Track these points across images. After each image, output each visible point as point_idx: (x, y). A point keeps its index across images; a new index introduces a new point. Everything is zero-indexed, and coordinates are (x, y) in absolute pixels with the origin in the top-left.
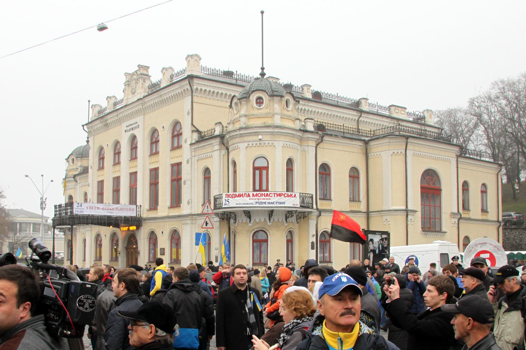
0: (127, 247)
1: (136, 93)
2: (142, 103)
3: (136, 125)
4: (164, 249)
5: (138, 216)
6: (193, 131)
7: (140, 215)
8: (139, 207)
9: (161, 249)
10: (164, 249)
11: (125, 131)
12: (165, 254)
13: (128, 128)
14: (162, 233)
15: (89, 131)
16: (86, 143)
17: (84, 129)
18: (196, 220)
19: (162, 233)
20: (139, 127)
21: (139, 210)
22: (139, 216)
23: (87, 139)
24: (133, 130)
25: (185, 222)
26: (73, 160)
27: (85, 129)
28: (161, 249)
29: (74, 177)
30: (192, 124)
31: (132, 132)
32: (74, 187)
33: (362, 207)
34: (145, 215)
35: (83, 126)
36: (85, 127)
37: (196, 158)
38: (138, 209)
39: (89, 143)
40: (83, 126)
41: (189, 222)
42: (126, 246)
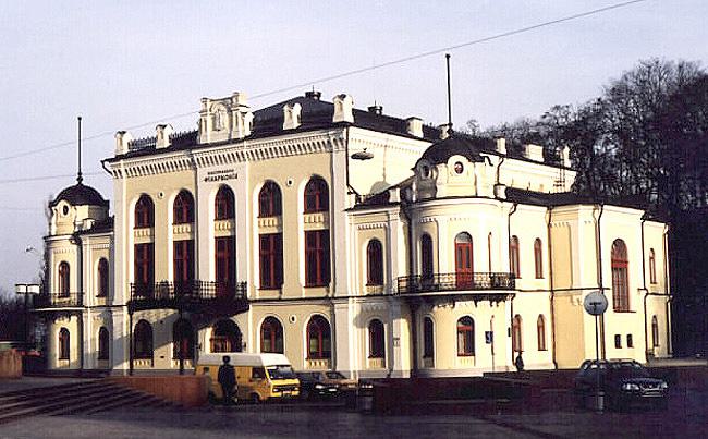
6: (349, 193)
30: (348, 185)
31: (220, 182)
33: (545, 284)
35: (103, 162)
36: (106, 163)
39: (83, 182)
40: (103, 162)
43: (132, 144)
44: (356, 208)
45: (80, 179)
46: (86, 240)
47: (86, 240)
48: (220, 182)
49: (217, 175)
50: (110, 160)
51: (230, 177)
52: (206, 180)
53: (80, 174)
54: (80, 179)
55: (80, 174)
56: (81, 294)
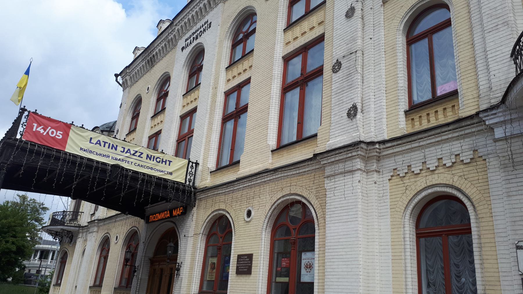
0: (153, 258)
4: (250, 257)
5: (188, 183)
7: (194, 183)
8: (194, 165)
9: (239, 257)
10: (250, 257)
12: (253, 269)
13: (189, 41)
14: (249, 213)
15: (123, 83)
17: (117, 80)
18: (379, 159)
19: (249, 213)
21: (193, 170)
22: (191, 184)
27: (118, 80)
28: (239, 257)
35: (116, 76)
38: (190, 170)
41: (359, 164)
42: (151, 255)
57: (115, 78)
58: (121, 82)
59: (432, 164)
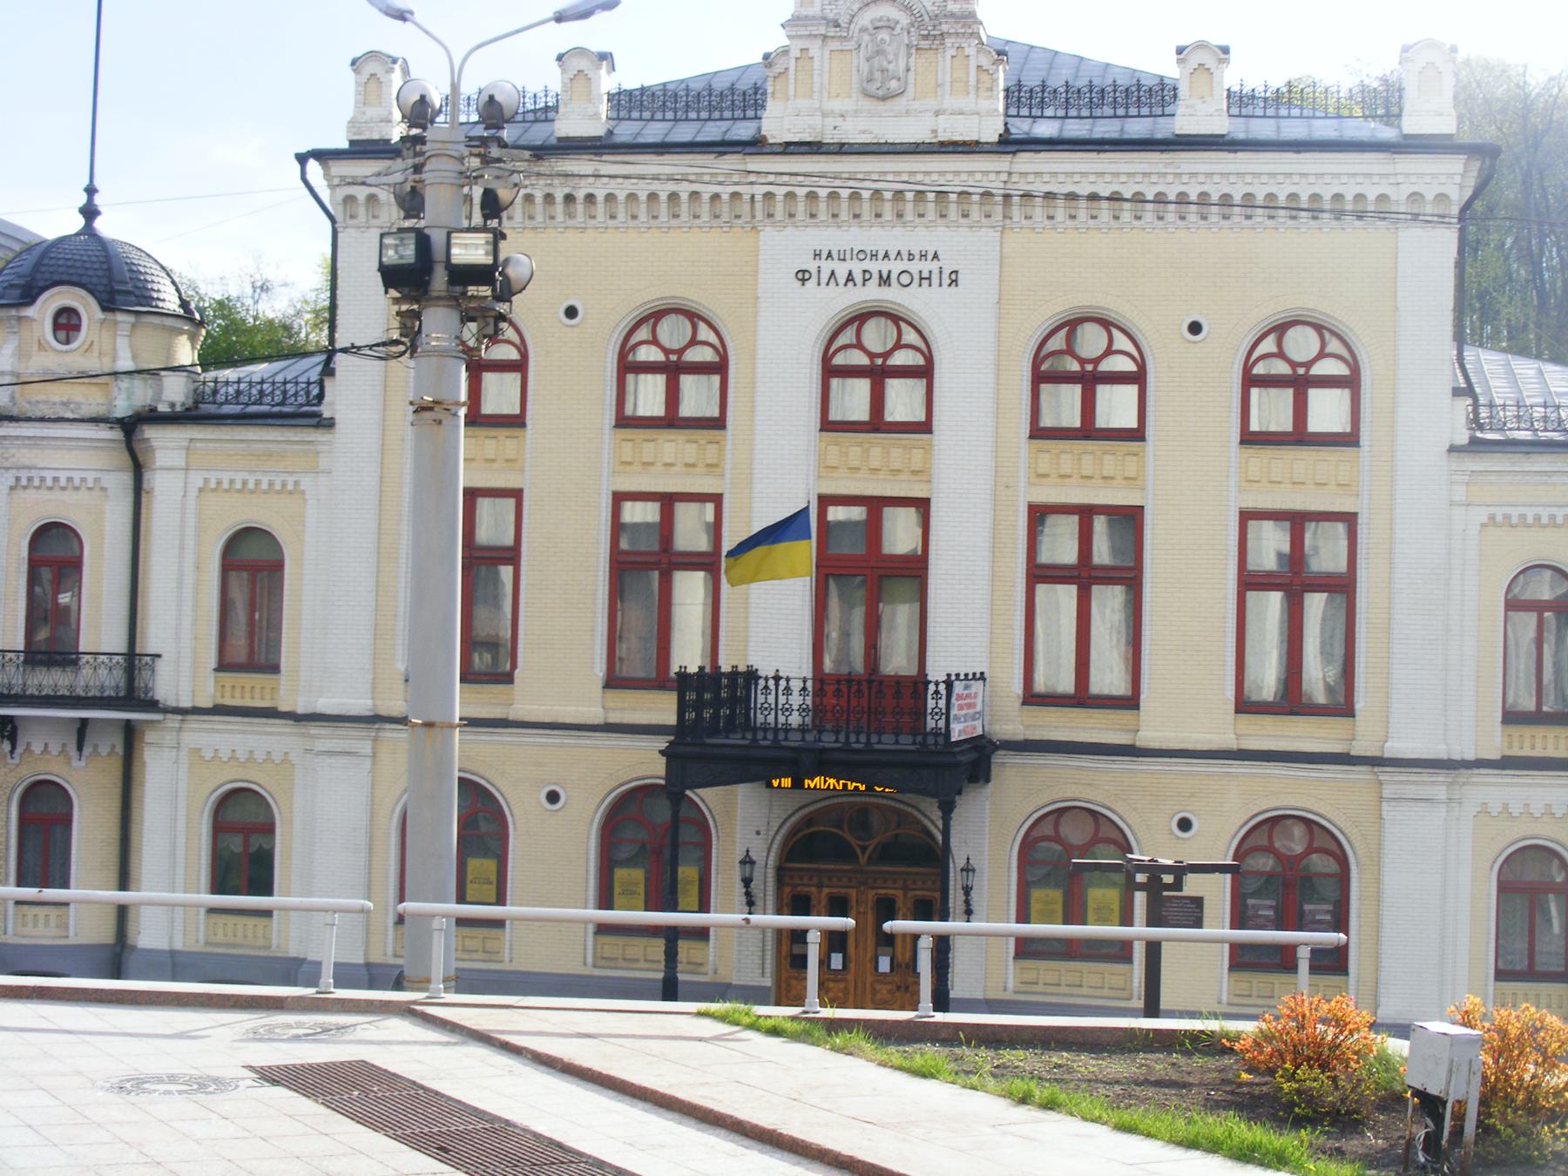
1: (900, 103)
2: (1010, 174)
3: (934, 266)
6: (1457, 392)
11: (803, 276)
16: (80, 222)
20: (954, 282)
23: (83, 198)
24: (885, 281)
25: (1411, 791)
26: (66, 323)
27: (309, 177)
29: (131, 426)
32: (96, 480)
34: (1015, 723)
35: (302, 159)
36: (313, 165)
37: (1481, 515)
39: (100, 225)
40: (302, 159)
43: (627, 102)
44: (1476, 446)
45: (90, 212)
46: (165, 444)
47: (165, 444)
48: (872, 294)
49: (857, 268)
50: (322, 156)
51: (925, 279)
52: (803, 276)
53: (91, 191)
54: (90, 212)
55: (91, 191)
56: (134, 660)
57: (297, 167)
58: (325, 195)
59: (1537, 808)
